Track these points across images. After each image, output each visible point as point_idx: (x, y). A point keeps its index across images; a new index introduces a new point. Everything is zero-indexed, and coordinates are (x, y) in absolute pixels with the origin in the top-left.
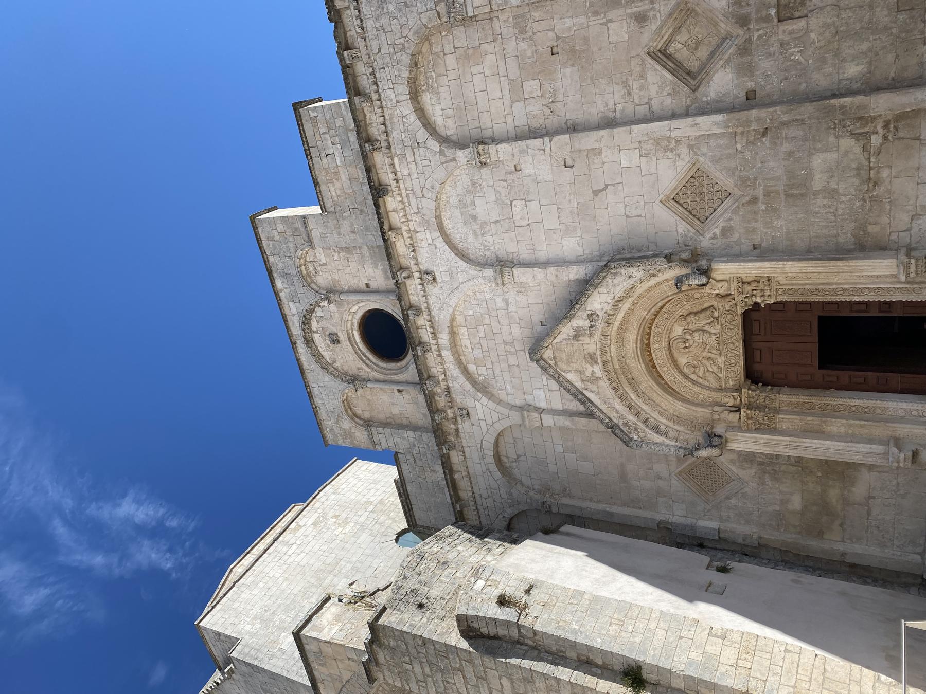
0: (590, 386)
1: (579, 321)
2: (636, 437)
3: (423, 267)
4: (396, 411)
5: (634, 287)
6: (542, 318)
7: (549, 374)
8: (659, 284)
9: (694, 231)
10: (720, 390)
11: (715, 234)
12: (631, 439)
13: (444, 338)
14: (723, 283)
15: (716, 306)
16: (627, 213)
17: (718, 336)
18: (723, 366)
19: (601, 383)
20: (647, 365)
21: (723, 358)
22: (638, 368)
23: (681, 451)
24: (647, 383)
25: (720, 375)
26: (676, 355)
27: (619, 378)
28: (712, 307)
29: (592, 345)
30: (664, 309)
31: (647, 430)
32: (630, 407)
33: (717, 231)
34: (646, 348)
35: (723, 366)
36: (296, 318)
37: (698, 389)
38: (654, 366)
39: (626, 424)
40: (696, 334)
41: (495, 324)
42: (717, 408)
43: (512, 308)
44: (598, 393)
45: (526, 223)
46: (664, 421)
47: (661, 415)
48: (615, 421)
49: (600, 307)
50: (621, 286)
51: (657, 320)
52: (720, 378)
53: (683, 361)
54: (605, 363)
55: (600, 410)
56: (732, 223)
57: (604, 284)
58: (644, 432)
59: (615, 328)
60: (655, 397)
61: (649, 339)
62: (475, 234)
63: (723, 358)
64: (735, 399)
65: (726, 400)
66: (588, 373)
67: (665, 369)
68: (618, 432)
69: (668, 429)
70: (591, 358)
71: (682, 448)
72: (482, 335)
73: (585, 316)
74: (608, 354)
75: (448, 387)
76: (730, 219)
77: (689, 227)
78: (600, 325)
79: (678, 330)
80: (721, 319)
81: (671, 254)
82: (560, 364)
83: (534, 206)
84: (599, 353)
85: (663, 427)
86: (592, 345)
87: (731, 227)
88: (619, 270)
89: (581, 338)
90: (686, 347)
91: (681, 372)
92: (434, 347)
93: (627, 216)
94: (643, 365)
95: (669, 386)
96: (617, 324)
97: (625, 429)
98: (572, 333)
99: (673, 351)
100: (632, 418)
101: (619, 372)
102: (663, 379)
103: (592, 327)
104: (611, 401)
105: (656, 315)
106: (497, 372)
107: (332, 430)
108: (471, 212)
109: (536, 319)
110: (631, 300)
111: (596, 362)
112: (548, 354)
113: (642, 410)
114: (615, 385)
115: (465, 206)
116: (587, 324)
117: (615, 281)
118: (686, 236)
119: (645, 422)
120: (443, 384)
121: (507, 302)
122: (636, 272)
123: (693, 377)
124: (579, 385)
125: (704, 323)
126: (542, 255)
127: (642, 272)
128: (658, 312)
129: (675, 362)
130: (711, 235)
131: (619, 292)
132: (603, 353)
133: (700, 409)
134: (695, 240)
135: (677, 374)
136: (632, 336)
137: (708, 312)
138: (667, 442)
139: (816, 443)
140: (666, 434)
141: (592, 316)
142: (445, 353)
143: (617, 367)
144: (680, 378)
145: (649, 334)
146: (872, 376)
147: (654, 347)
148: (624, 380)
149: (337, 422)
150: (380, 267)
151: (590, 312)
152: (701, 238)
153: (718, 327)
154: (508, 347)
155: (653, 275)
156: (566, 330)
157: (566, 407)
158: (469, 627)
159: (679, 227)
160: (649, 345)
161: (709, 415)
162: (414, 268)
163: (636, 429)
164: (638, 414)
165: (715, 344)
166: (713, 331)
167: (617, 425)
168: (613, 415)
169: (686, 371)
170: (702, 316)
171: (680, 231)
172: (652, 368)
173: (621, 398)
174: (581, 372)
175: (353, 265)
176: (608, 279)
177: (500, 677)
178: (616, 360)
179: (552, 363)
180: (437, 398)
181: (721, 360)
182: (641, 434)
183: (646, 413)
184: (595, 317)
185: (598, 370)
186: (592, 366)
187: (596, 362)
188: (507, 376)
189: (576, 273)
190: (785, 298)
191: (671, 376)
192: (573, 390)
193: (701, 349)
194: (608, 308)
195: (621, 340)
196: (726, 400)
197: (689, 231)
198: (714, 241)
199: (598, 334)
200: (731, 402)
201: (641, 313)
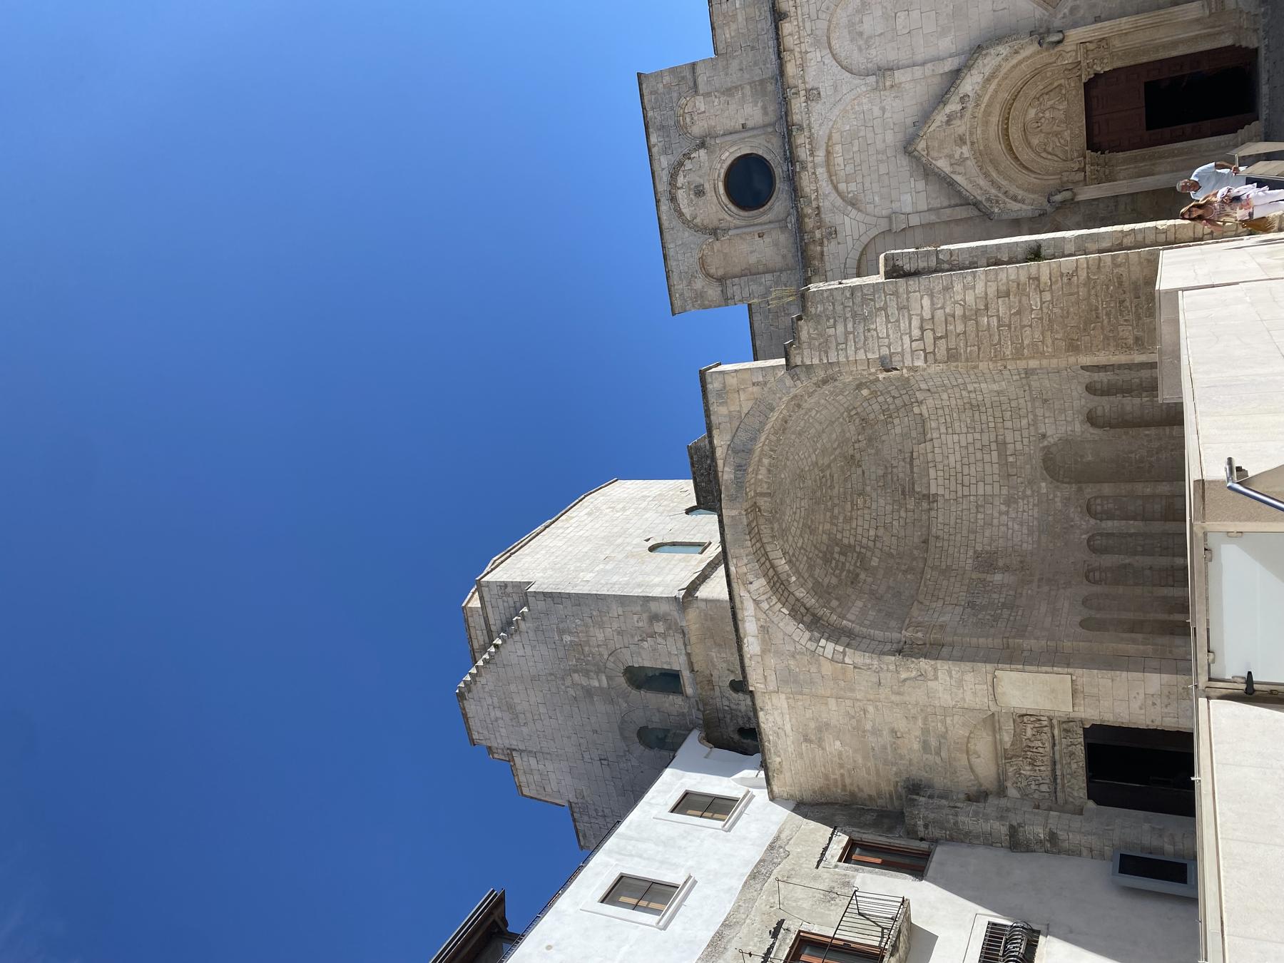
0: (958, 169)
1: (953, 106)
3: (809, 86)
4: (753, 259)
6: (915, 119)
8: (1020, 63)
13: (821, 154)
17: (1066, 112)
19: (968, 162)
22: (998, 147)
27: (983, 157)
28: (1060, 85)
29: (960, 127)
32: (993, 182)
36: (665, 172)
37: (1048, 163)
39: (988, 200)
41: (870, 135)
43: (887, 115)
54: (972, 143)
58: (1005, 203)
62: (860, 49)
66: (957, 156)
70: (961, 140)
72: (855, 149)
73: (958, 99)
75: (818, 208)
78: (970, 105)
79: (1032, 113)
83: (915, 14)
86: (960, 127)
92: (810, 165)
96: (983, 106)
100: (993, 191)
106: (867, 185)
107: (682, 294)
108: (858, 29)
109: (909, 121)
111: (965, 143)
115: (854, 24)
116: (959, 107)
120: (814, 204)
121: (883, 110)
122: (1003, 50)
124: (947, 169)
126: (919, 57)
129: (1029, 144)
131: (987, 71)
132: (971, 134)
138: (1024, 207)
139: (1149, 179)
140: (1023, 201)
141: (963, 99)
142: (820, 171)
144: (1033, 156)
145: (1008, 119)
146: (1188, 127)
147: (1012, 130)
149: (689, 284)
150: (760, 104)
154: (880, 157)
155: (1017, 52)
158: (894, 265)
162: (801, 86)
164: (999, 188)
171: (1037, 16)
174: (950, 156)
175: (732, 107)
177: (922, 298)
180: (807, 220)
181: (1067, 134)
185: (966, 150)
187: (965, 143)
188: (876, 187)
190: (1119, 64)
191: (1025, 155)
195: (986, 123)
199: (968, 114)
200: (1076, 166)
201: (1005, 95)
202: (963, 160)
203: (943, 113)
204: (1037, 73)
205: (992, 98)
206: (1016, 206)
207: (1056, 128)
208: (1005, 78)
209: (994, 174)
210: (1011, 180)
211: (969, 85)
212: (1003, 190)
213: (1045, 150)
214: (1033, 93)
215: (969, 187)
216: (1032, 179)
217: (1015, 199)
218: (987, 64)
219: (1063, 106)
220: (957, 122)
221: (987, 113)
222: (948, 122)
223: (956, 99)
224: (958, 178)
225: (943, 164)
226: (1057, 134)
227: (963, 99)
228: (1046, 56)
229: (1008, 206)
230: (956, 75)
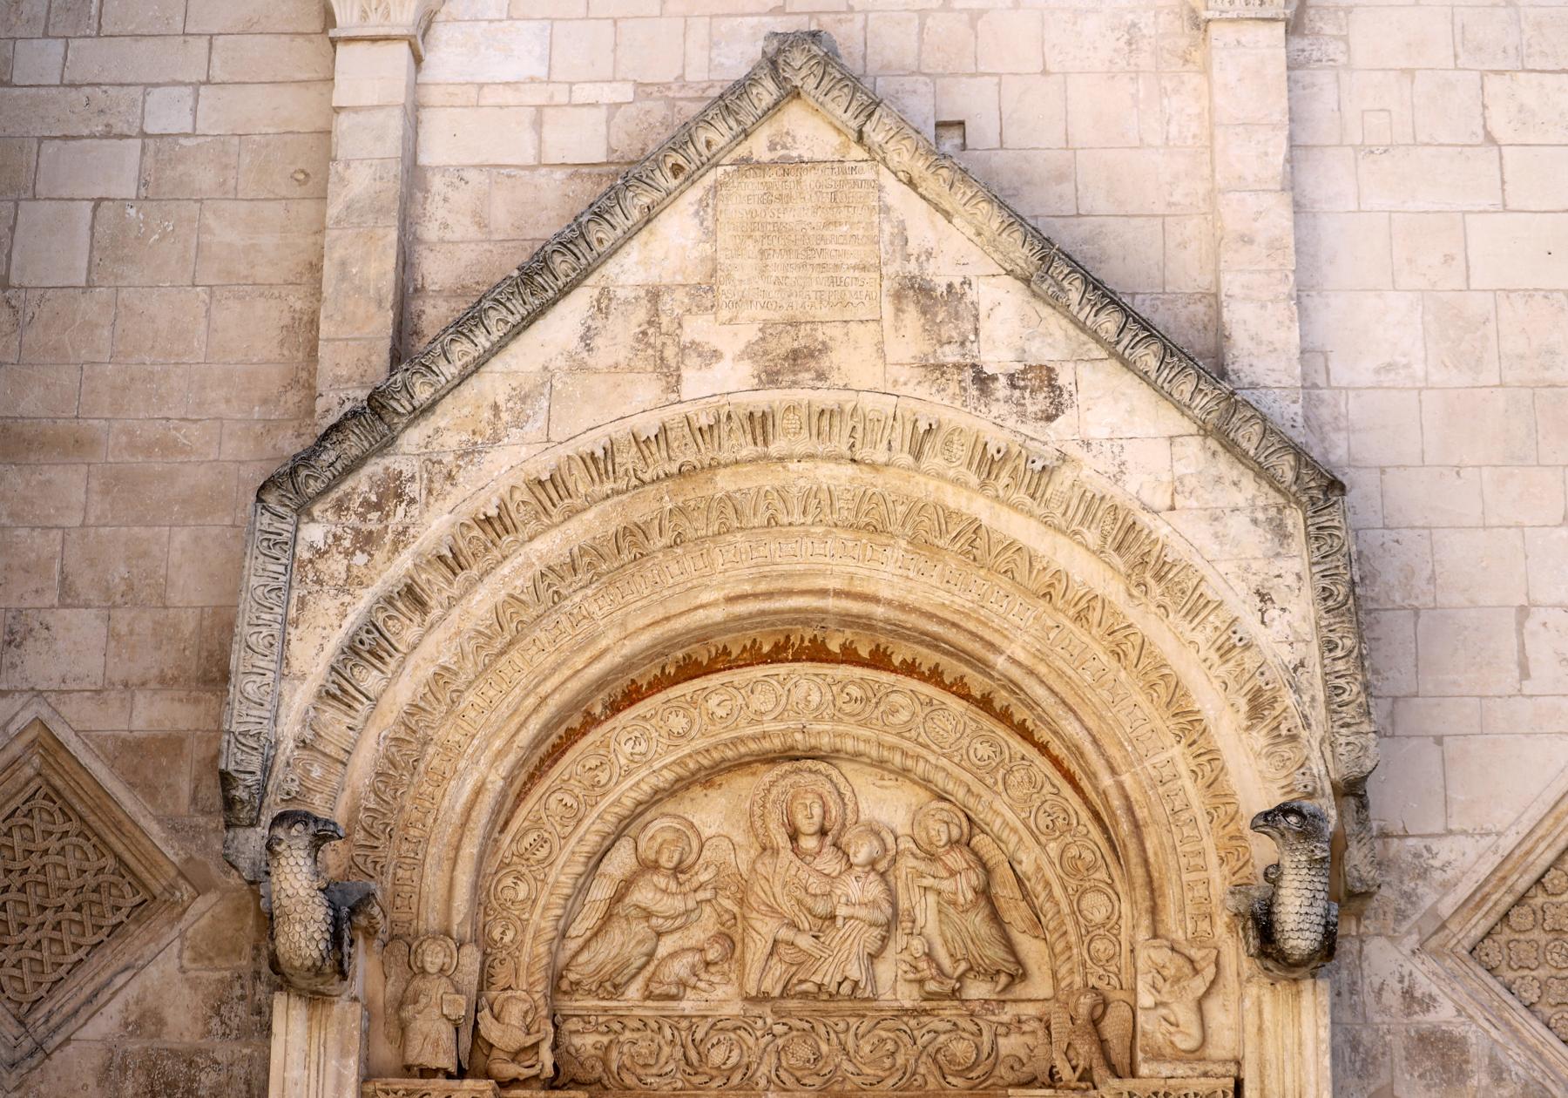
0: (620, 333)
1: (1010, 325)
2: (314, 533)
5: (1197, 608)
6: (982, 130)
7: (703, 119)
8: (1190, 725)
9: (1447, 907)
10: (558, 983)
11: (1428, 1003)
12: (303, 510)
14: (1195, 1031)
15: (1020, 991)
16: (1538, 616)
17: (857, 997)
18: (688, 1005)
19: (647, 390)
20: (703, 635)
21: (734, 1008)
22: (707, 587)
23: (255, 763)
24: (619, 625)
25: (634, 991)
26: (744, 786)
27: (660, 481)
28: (1019, 974)
29: (875, 363)
30: (1018, 746)
31: (364, 599)
32: (495, 524)
33: (1444, 1014)
34: (795, 643)
35: (688, 1005)
37: (564, 874)
38: (690, 670)
39: (392, 492)
40: (875, 889)
42: (470, 959)
44: (579, 367)
45: (1501, 131)
46: (404, 691)
47: (442, 676)
48: (412, 438)
49: (1096, 432)
50: (1212, 549)
51: (956, 705)
52: (618, 989)
53: (714, 815)
54: (760, 424)
55: (478, 365)
56: (1480, 1079)
57: (1224, 465)
58: (352, 581)
59: (954, 499)
60: (521, 665)
61: (849, 656)
63: (734, 1008)
64: (516, 1056)
65: (514, 1014)
66: (698, 328)
67: (678, 723)
68: (353, 444)
69: (363, 708)
70: (793, 358)
71: (267, 769)
73: (1041, 353)
74: (803, 445)
76: (1498, 1073)
77: (1464, 891)
78: (994, 423)
79: (887, 806)
80: (949, 1010)
81: (1363, 805)
82: (752, 185)
84: (825, 398)
85: (370, 679)
86: (875, 363)
87: (1462, 1075)
88: (1298, 544)
89: (912, 314)
90: (794, 836)
91: (657, 797)
93: (1523, 612)
94: (718, 614)
95: (572, 737)
96: (980, 507)
97: (361, 484)
98: (941, 274)
99: (768, 775)
100: (435, 525)
101: (692, 492)
102: (614, 708)
103: (983, 381)
104: (534, 429)
105: (985, 703)
109: (972, 101)
110: (1112, 588)
112: (810, 130)
113: (472, 585)
114: (627, 458)
116: (997, 358)
117: (1238, 525)
118: (1424, 874)
119: (412, 596)
122: (1290, 630)
123: (621, 861)
124: (628, 271)
125: (932, 928)
126: (1333, 181)
127: (1289, 656)
128: (1004, 717)
129: (706, 776)
130: (1424, 985)
131: (1180, 534)
133: (464, 879)
134: (1401, 915)
135: (645, 781)
136: (892, 579)
137: (996, 953)
138: (299, 698)
141: (1042, 385)
143: (725, 482)
144: (627, 793)
145: (879, 660)
147: (806, 684)
148: (642, 509)
151: (1064, 379)
152: (1412, 941)
153: (908, 996)
155: (1258, 706)
156: (956, 243)
157: (437, 183)
159: (1468, 844)
160: (817, 653)
161: (432, 920)
163: (366, 541)
164: (452, 562)
165: (827, 975)
166: (886, 970)
167: (386, 444)
168: (447, 428)
169: (659, 826)
170: (978, 922)
171: (1445, 850)
172: (690, 662)
173: (549, 489)
174: (705, 293)
176: (1248, 491)
178: (767, 479)
179: (758, 146)
181: (721, 997)
182: (336, 565)
183: (452, 602)
184: (1040, 402)
185: (724, 381)
186: (749, 353)
187: (770, 378)
189: (1263, 343)
192: (601, 234)
193: (786, 905)
194: (1091, 472)
195: (870, 525)
196: (514, 1014)
197: (1448, 887)
198: (1392, 999)
199: (945, 406)
200: (504, 1033)
201: (1019, 636)
202: (665, 361)
203: (980, 264)
204: (1117, 834)
205: (1008, 563)
206: (315, 649)
207: (765, 929)
208: (1123, 644)
209: (550, 545)
210: (504, 635)
211: (1123, 429)
212: (436, 586)
213: (649, 867)
214: (1001, 812)
215: (493, 384)
216: (475, 771)
217: (368, 646)
218: (1226, 532)
219: (893, 984)
220: (908, 338)
221: (932, 533)
222: (917, 292)
223: (1052, 339)
224: (564, 324)
225: (669, 245)
226: (730, 942)
227: (1042, 385)
228: (1202, 884)
229: (327, 604)
230: (1187, 355)
